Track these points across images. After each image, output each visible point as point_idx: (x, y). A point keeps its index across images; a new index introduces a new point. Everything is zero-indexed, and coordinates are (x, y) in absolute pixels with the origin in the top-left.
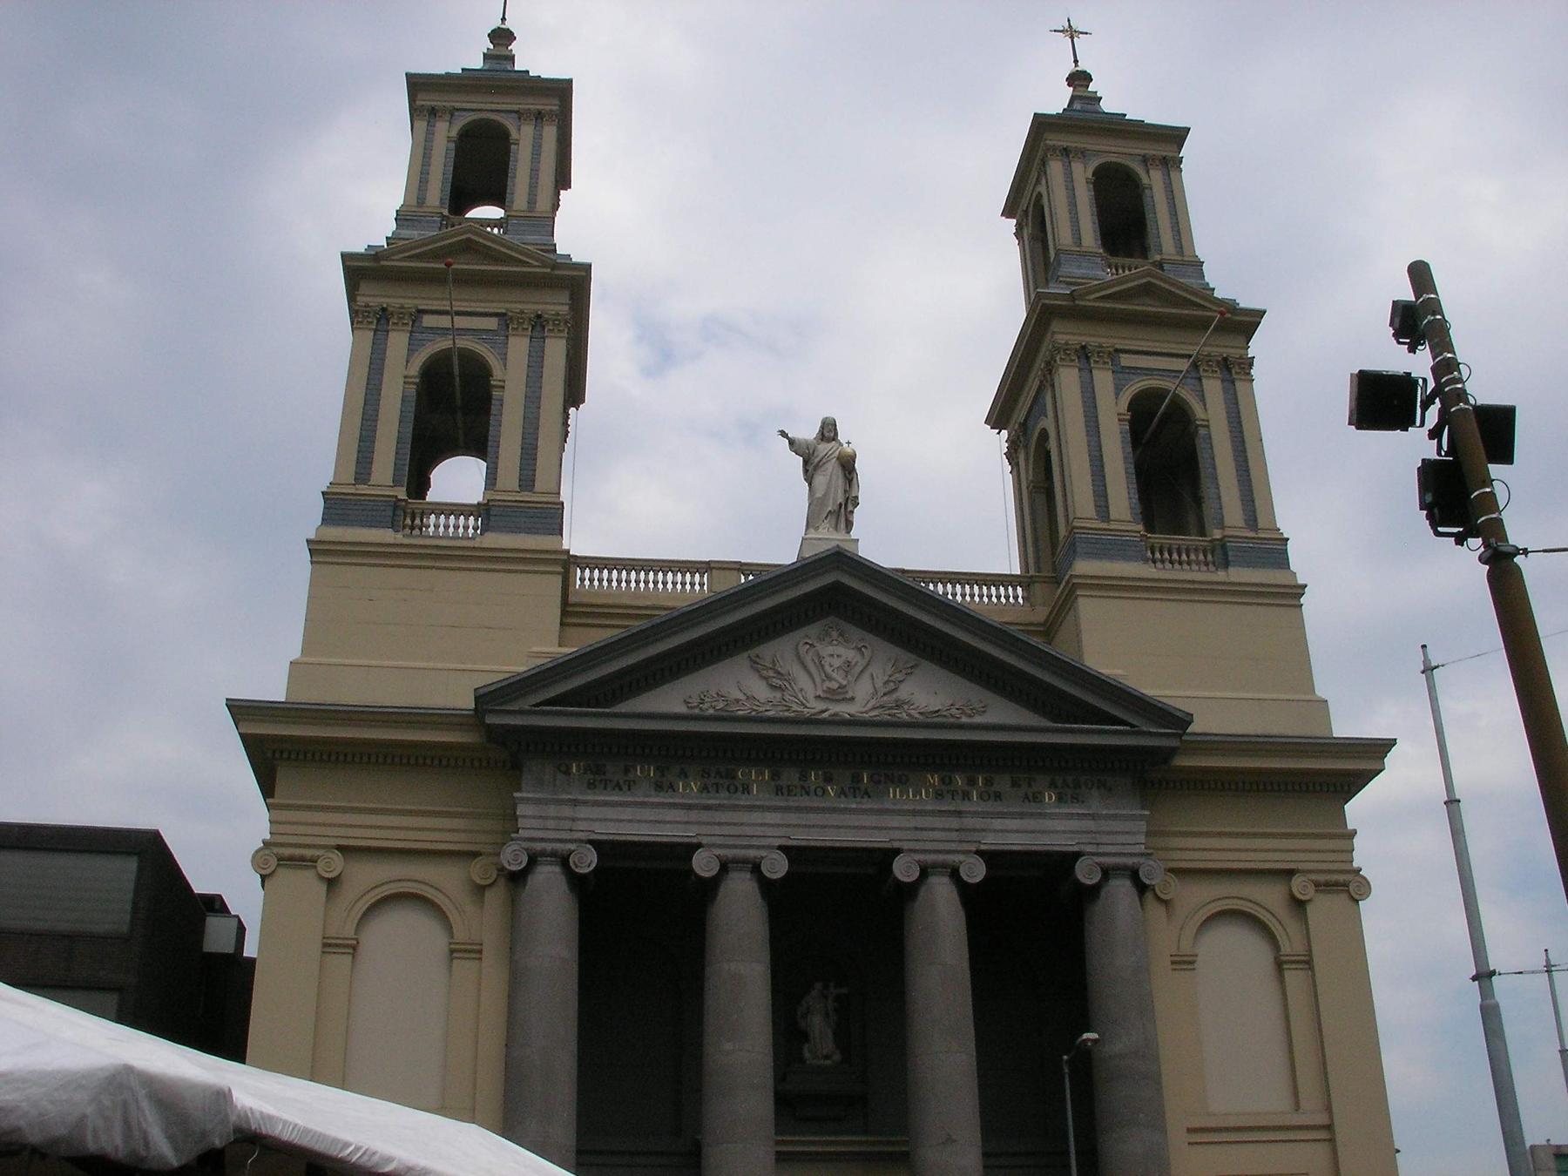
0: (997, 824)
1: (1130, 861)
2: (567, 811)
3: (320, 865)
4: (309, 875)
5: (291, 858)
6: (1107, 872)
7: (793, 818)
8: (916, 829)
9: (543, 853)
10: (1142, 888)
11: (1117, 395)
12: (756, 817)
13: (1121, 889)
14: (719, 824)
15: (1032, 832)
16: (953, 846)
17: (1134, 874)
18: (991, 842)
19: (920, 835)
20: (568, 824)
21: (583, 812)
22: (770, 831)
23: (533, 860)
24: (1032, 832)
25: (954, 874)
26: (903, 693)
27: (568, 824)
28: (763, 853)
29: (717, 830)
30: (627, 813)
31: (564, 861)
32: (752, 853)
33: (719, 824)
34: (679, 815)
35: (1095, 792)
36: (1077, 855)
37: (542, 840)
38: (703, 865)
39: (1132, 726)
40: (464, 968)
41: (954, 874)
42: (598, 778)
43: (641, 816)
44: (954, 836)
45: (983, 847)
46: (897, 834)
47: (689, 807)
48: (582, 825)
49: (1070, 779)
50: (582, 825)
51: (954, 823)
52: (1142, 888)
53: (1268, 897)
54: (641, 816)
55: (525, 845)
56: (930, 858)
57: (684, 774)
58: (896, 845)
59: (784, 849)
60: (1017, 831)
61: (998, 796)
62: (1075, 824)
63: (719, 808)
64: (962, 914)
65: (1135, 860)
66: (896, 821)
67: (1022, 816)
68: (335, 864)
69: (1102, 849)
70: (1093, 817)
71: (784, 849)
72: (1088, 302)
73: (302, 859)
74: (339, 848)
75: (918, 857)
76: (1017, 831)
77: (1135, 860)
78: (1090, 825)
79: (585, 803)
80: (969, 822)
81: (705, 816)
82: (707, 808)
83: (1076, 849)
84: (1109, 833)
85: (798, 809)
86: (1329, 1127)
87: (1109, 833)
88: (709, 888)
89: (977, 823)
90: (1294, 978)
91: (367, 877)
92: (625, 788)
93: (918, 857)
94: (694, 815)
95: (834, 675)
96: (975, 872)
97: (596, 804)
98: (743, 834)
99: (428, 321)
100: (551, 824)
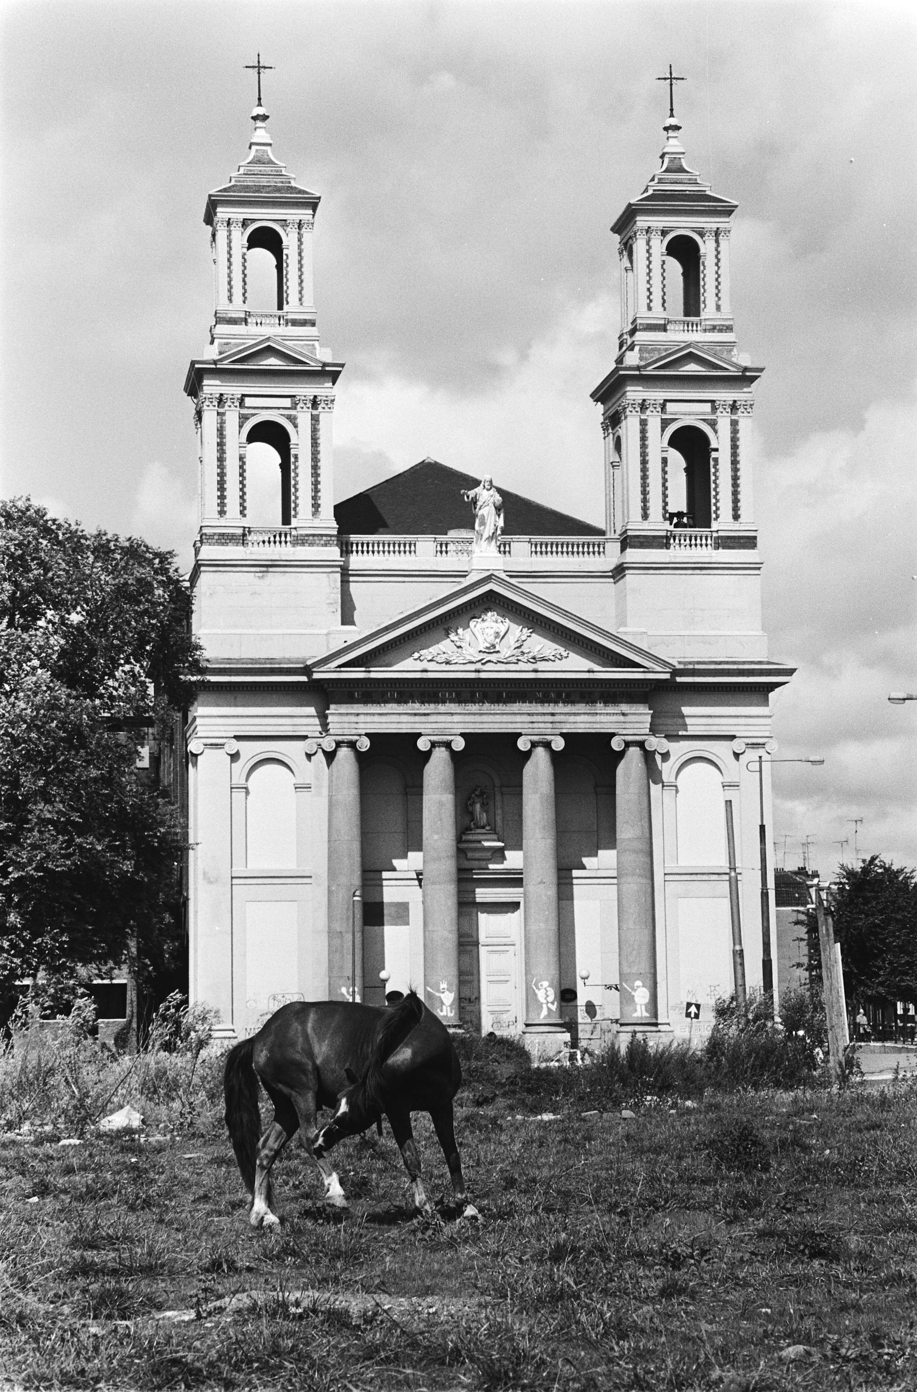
0: (572, 719)
3: (226, 747)
5: (211, 745)
6: (628, 744)
9: (343, 742)
11: (663, 431)
13: (634, 753)
17: (641, 745)
21: (362, 718)
29: (429, 726)
31: (352, 745)
32: (445, 738)
40: (305, 794)
44: (550, 726)
45: (564, 731)
46: (519, 725)
48: (361, 726)
50: (361, 726)
51: (550, 718)
53: (720, 751)
55: (334, 737)
59: (462, 735)
62: (615, 718)
66: (518, 718)
68: (234, 746)
71: (462, 735)
72: (649, 371)
73: (217, 745)
74: (236, 737)
80: (557, 718)
81: (423, 719)
88: (427, 755)
91: (250, 751)
94: (417, 719)
99: (248, 402)
100: (346, 725)
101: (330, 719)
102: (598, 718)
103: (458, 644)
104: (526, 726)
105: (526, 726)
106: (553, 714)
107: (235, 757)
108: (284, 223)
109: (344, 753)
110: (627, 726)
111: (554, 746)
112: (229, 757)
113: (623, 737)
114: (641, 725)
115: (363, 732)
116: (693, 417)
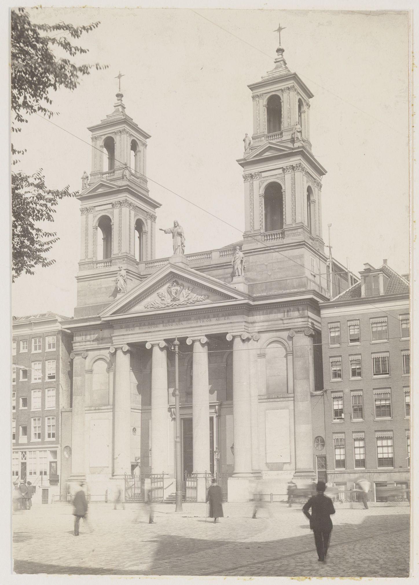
3: (83, 355)
16: (200, 335)
19: (193, 332)
23: (116, 350)
28: (160, 341)
38: (148, 346)
39: (236, 299)
43: (136, 336)
44: (200, 332)
54: (136, 336)
59: (165, 340)
69: (234, 331)
71: (165, 340)
86: (294, 397)
90: (290, 358)
98: (155, 337)
101: (113, 338)
103: (163, 298)
104: (189, 333)
105: (189, 333)
108: (115, 133)
109: (119, 353)
113: (232, 334)
115: (126, 343)
116: (275, 177)
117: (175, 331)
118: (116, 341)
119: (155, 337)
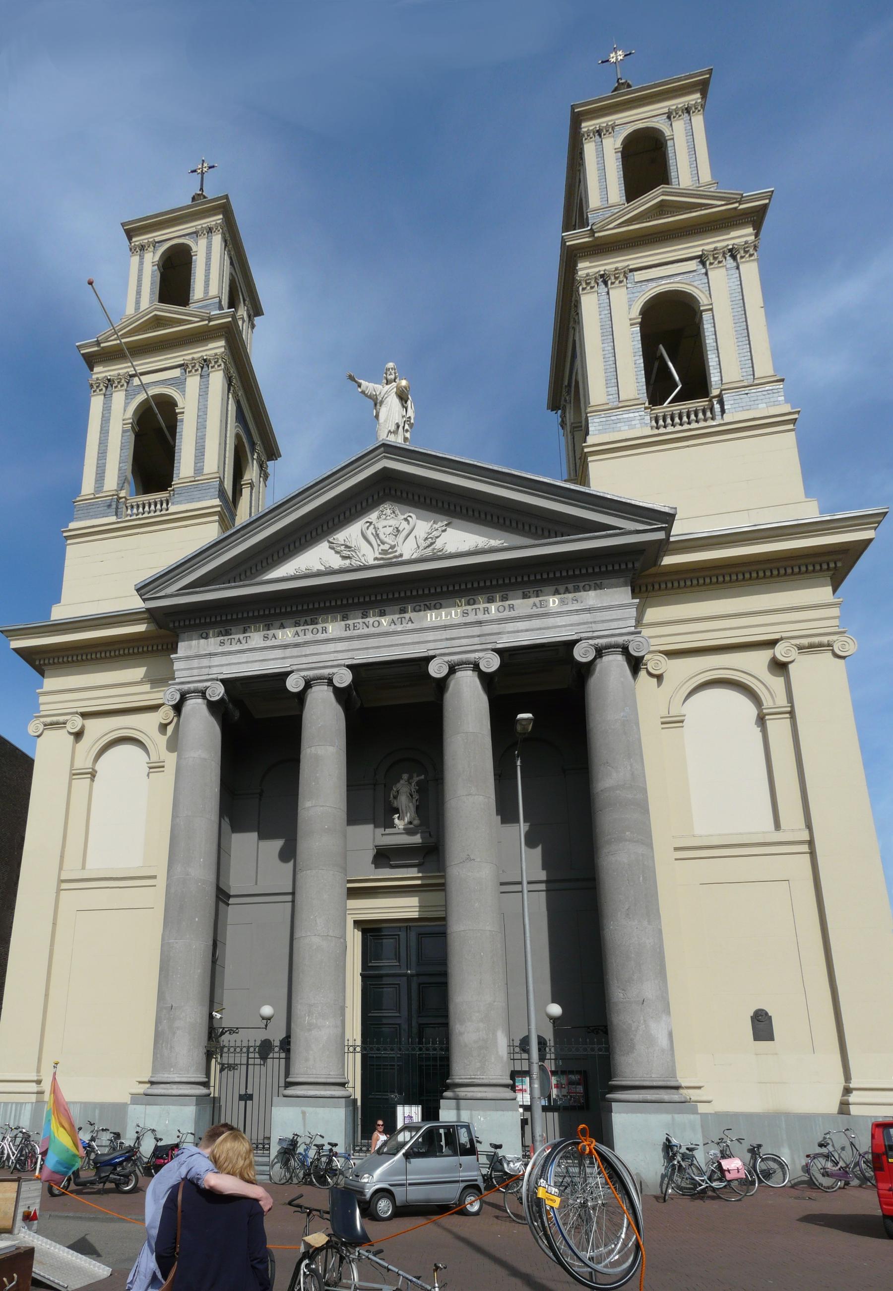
0: (510, 627)
1: (620, 640)
2: (205, 662)
4: (63, 732)
7: (356, 644)
8: (447, 639)
10: (635, 664)
12: (331, 647)
14: (306, 656)
15: (540, 629)
18: (505, 641)
20: (206, 671)
21: (216, 661)
22: (340, 656)
24: (540, 629)
25: (476, 667)
26: (439, 544)
27: (206, 671)
30: (244, 657)
33: (306, 656)
34: (278, 653)
35: (592, 593)
36: (574, 642)
37: (189, 682)
41: (476, 667)
42: (226, 638)
44: (476, 640)
46: (431, 646)
47: (285, 647)
48: (215, 670)
49: (570, 586)
51: (476, 630)
52: (635, 664)
56: (455, 658)
57: (282, 627)
58: (431, 653)
60: (527, 630)
61: (512, 607)
62: (575, 618)
63: (306, 644)
64: (484, 699)
65: (626, 638)
66: (430, 636)
67: (530, 617)
69: (596, 634)
70: (589, 610)
75: (447, 658)
76: (527, 630)
77: (626, 638)
78: (587, 617)
79: (215, 654)
80: (487, 629)
82: (297, 645)
83: (574, 637)
84: (603, 621)
85: (360, 637)
87: (603, 621)
89: (494, 628)
92: (244, 642)
93: (447, 658)
94: (288, 652)
95: (386, 540)
96: (491, 663)
97: (223, 654)
100: (195, 672)
101: (177, 665)
102: (550, 621)
106: (480, 623)
107: (78, 735)
110: (595, 627)
111: (483, 667)
112: (72, 737)
113: (591, 642)
114: (621, 624)
117: (388, 638)
118: (185, 673)
119: (319, 656)
